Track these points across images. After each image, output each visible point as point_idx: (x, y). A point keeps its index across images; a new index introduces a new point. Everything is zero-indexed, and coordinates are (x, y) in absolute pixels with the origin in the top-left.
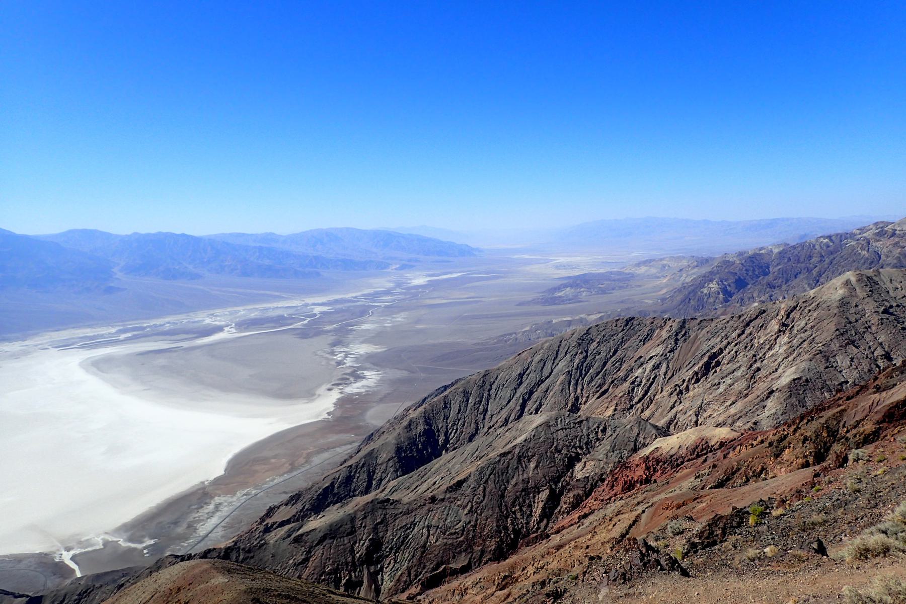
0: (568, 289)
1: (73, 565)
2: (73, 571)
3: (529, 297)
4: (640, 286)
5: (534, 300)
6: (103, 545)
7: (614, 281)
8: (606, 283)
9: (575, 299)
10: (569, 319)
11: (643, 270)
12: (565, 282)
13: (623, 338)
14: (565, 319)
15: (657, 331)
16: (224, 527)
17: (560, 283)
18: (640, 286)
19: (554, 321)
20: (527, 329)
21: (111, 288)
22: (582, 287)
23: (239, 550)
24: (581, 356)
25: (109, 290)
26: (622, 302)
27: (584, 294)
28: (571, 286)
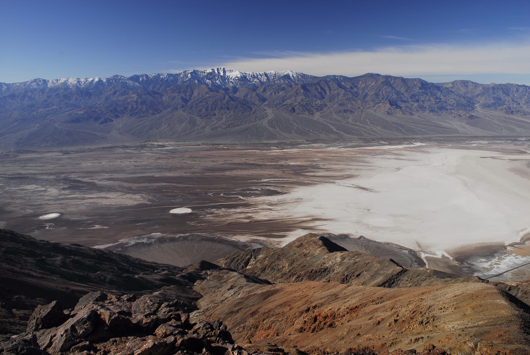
1: (425, 261)
2: (425, 264)
6: (442, 257)
16: (513, 273)
21: (472, 116)
23: (519, 290)
25: (471, 117)
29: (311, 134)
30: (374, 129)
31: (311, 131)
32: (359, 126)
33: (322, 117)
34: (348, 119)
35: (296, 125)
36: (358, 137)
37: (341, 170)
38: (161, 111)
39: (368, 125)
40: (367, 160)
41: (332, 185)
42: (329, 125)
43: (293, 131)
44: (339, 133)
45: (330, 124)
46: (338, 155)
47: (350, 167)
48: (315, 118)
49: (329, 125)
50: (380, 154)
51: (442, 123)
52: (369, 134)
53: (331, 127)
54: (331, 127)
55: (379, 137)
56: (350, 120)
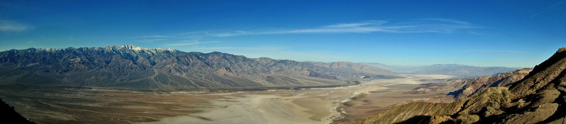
0: (422, 88)
3: (408, 91)
4: (447, 88)
5: (409, 92)
7: (439, 86)
8: (436, 87)
9: (424, 92)
10: (419, 99)
11: (450, 82)
12: (422, 86)
13: (415, 109)
14: (417, 100)
15: (427, 107)
17: (420, 86)
18: (447, 88)
19: (414, 100)
20: (404, 102)
22: (427, 88)
24: (399, 116)
25: (268, 77)
26: (439, 94)
27: (427, 91)
28: (424, 88)
29: (179, 85)
30: (216, 83)
31: (179, 84)
32: (208, 81)
33: (187, 76)
34: (202, 77)
35: (171, 80)
36: (206, 88)
37: (193, 107)
38: (93, 68)
39: (213, 81)
40: (209, 101)
41: (186, 117)
42: (190, 81)
43: (168, 84)
44: (196, 86)
45: (191, 80)
46: (193, 98)
47: (199, 106)
48: (183, 77)
49: (190, 81)
50: (218, 98)
51: (253, 80)
52: (213, 86)
53: (192, 82)
54: (192, 82)
55: (219, 88)
56: (203, 78)
